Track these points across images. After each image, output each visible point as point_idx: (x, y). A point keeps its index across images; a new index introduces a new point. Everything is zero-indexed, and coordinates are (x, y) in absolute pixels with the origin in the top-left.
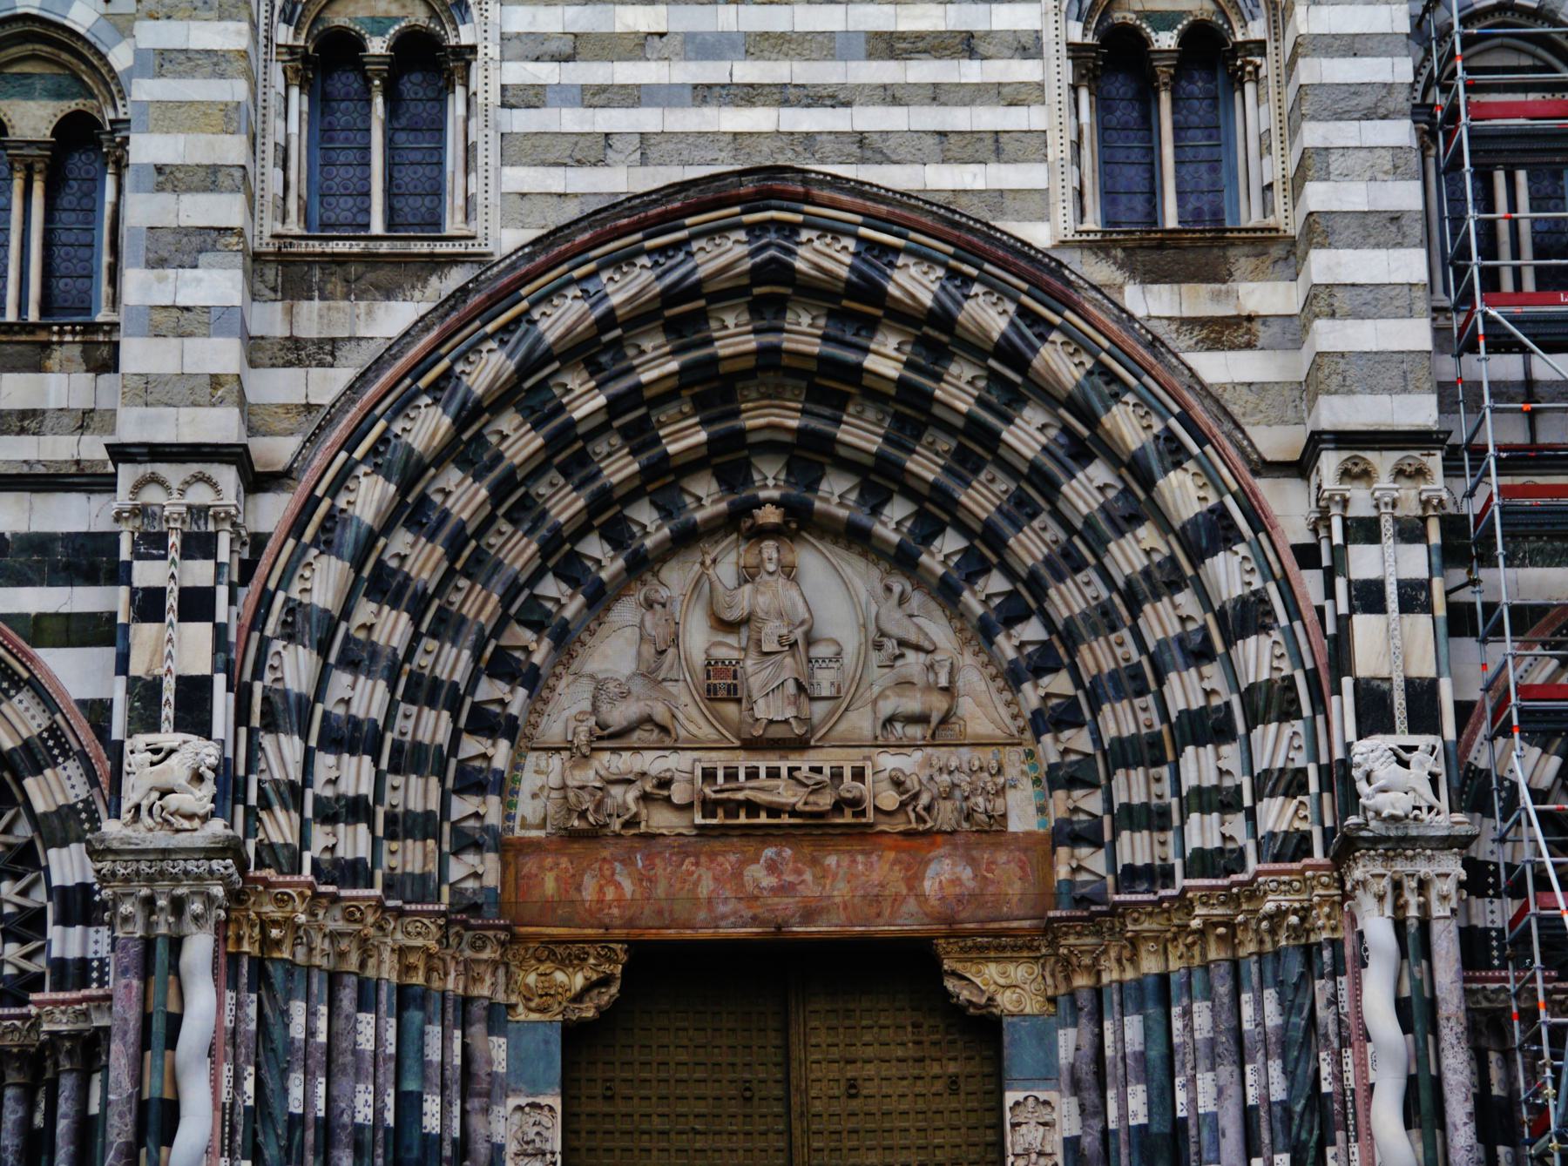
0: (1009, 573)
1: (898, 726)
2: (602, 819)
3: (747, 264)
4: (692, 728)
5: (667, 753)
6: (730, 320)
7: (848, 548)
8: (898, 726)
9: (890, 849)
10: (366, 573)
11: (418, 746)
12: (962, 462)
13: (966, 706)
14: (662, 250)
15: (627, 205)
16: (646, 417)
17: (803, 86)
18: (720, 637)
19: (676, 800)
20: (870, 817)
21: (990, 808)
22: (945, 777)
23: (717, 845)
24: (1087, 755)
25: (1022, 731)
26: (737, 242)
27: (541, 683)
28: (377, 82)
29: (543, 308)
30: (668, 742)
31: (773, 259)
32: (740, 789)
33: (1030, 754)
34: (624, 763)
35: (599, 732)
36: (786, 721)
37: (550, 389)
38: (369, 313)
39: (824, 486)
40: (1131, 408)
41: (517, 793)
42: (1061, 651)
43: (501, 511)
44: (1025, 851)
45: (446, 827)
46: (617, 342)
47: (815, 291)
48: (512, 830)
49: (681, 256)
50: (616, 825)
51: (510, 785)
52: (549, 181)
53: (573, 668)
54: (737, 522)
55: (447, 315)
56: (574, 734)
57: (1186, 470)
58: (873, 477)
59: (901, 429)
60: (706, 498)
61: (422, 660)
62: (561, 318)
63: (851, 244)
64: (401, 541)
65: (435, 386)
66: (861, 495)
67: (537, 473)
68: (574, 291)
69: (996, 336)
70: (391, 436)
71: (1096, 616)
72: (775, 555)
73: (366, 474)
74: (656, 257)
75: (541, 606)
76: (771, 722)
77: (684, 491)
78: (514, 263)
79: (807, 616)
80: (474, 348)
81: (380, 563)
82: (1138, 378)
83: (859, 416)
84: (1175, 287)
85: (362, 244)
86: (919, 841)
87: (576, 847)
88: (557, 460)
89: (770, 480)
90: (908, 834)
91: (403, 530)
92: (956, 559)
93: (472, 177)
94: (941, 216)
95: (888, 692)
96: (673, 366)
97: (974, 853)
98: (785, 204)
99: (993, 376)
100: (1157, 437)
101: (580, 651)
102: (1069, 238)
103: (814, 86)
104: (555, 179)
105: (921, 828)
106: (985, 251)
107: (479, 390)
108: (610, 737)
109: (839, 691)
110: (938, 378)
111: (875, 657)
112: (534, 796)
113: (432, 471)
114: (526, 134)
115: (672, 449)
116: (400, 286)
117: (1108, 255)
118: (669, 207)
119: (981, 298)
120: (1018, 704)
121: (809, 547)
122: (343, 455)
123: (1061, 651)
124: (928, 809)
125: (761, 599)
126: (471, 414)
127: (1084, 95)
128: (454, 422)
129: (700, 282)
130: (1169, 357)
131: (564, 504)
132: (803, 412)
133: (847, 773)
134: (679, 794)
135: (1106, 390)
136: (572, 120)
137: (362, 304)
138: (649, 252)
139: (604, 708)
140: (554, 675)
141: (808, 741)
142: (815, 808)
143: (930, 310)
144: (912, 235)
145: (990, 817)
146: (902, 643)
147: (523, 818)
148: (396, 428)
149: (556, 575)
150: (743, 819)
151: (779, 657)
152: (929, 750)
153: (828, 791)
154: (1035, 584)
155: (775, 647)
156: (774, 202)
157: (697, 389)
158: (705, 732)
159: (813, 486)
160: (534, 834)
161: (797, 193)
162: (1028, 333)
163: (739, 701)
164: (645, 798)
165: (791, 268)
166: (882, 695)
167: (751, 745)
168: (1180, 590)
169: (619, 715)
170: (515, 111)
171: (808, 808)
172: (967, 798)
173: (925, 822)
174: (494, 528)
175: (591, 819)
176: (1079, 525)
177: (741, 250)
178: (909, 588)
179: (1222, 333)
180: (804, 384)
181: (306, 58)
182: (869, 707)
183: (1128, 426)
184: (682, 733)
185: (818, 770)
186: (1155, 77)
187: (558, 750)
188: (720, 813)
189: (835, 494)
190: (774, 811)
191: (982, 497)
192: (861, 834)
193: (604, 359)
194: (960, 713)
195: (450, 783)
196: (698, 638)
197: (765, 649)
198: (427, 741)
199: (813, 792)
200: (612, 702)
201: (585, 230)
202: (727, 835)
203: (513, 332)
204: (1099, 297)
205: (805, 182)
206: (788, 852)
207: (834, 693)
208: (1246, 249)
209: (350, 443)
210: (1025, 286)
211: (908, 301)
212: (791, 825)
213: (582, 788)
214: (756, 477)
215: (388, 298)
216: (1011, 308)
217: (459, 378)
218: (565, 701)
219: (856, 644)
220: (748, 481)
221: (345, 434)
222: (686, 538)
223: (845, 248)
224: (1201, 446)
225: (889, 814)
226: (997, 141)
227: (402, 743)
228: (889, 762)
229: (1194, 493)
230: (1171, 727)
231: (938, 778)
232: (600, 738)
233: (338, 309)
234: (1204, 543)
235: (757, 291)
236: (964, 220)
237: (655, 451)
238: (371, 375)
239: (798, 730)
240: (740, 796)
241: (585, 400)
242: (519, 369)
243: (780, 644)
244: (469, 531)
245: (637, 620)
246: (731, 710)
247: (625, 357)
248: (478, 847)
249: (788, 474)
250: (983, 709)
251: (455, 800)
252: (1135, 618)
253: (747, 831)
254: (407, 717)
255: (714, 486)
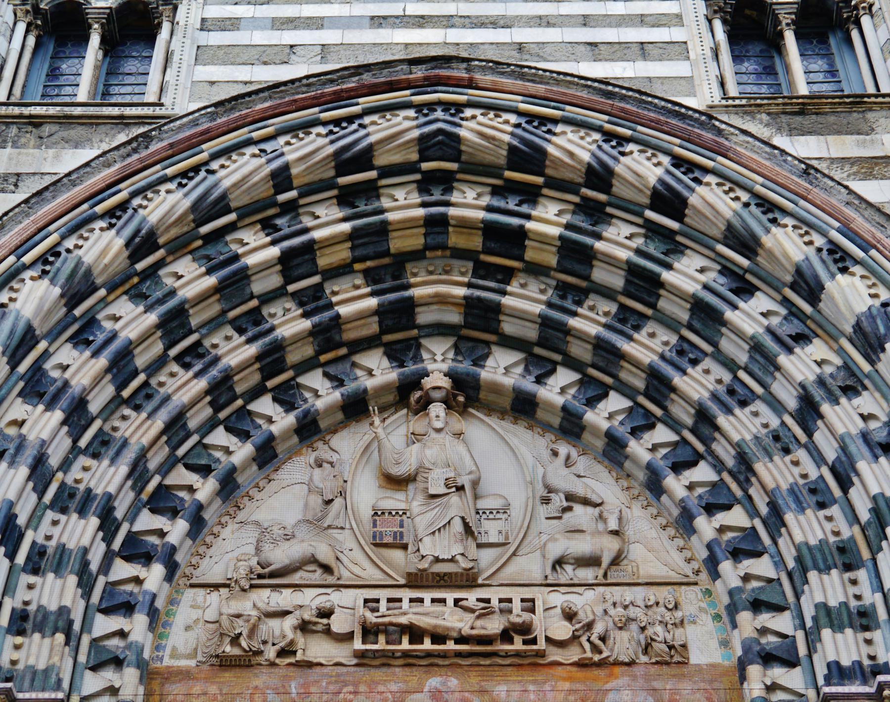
0: (673, 424)
1: (569, 568)
2: (256, 645)
3: (416, 133)
4: (357, 570)
5: (329, 591)
6: (400, 194)
7: (515, 423)
8: (569, 568)
9: (564, 679)
10: (23, 368)
11: (62, 549)
12: (623, 321)
13: (636, 552)
14: (337, 122)
15: (305, 81)
16: (318, 289)
17: (468, 17)
18: (389, 493)
19: (335, 628)
20: (542, 644)
21: (669, 637)
22: (620, 610)
23: (378, 674)
24: (770, 581)
25: (697, 572)
26: (406, 118)
27: (205, 530)
28: (96, 26)
29: (222, 161)
30: (331, 580)
31: (440, 131)
32: (405, 614)
33: (708, 593)
34: (284, 599)
35: (260, 570)
36: (452, 560)
37: (226, 244)
38: (57, 157)
39: (490, 362)
40: (790, 229)
41: (170, 625)
42: (734, 486)
43: (173, 352)
44: (711, 682)
45: (86, 640)
46: (291, 208)
47: (477, 169)
48: (161, 659)
49: (354, 126)
50: (271, 653)
51: (163, 618)
52: (237, 74)
53: (241, 516)
54: (407, 395)
55: (129, 155)
56: (236, 569)
57: (853, 274)
58: (538, 350)
59: (563, 297)
60: (377, 371)
61: (75, 472)
62: (242, 172)
63: (513, 118)
64: (66, 354)
65: (111, 213)
66: (527, 369)
67: (213, 324)
68: (254, 150)
69: (652, 181)
70: (61, 249)
71: (769, 441)
72: (442, 414)
73: (32, 279)
74: (331, 127)
75: (210, 455)
76: (437, 560)
77: (354, 365)
78: (197, 119)
79: (474, 468)
80: (153, 186)
81: (37, 368)
82: (796, 205)
83: (523, 286)
84: (821, 138)
85: (58, 108)
86: (596, 672)
87: (228, 675)
88: (232, 314)
89: (438, 362)
90: (582, 664)
91: (69, 346)
92: (620, 418)
93: (168, 70)
94: (595, 88)
95: (557, 536)
96: (346, 227)
97: (656, 684)
98: (451, 89)
99: (653, 230)
100: (819, 250)
101: (248, 504)
102: (716, 103)
103: (477, 17)
104: (243, 73)
105: (597, 658)
106: (638, 115)
107: (153, 219)
108: (271, 576)
109: (507, 538)
110: (599, 237)
111: (543, 511)
112: (188, 628)
113: (102, 292)
114: (219, 47)
115: (344, 310)
116: (90, 140)
117: (754, 118)
118: (344, 87)
119: (636, 155)
120: (690, 549)
121: (476, 422)
122: (12, 259)
123: (734, 486)
124: (603, 639)
125: (428, 452)
126: (142, 244)
127: (718, 25)
128: (127, 245)
129: (370, 148)
130: (826, 180)
131: (235, 352)
132: (469, 285)
133: (517, 606)
134: (338, 624)
135: (764, 218)
136: (260, 37)
137: (51, 152)
138: (324, 124)
139: (266, 547)
140: (220, 523)
141: (475, 579)
142: (483, 632)
143: (589, 164)
144: (568, 108)
145: (671, 647)
146: (570, 497)
147: (174, 649)
148: (69, 243)
149: (228, 429)
150: (405, 645)
151: (446, 499)
152: (601, 589)
153: (496, 617)
154: (704, 420)
155: (442, 490)
156: (440, 88)
157: (369, 264)
158: (372, 575)
159: (479, 361)
160: (183, 663)
161: (462, 79)
162: (685, 178)
163: (405, 547)
164: (304, 627)
165: (457, 138)
166: (552, 539)
167: (416, 580)
168: (857, 393)
169: (280, 555)
170: (210, 33)
171: (474, 632)
172: (643, 629)
173: (600, 652)
174: (166, 370)
175: (244, 644)
176: (742, 358)
177: (408, 124)
178: (574, 453)
179: (873, 168)
180: (470, 265)
181: (36, 10)
182: (538, 553)
183: (787, 244)
184: (346, 574)
185: (488, 601)
186: (778, 22)
187: (216, 587)
188: (382, 638)
189: (501, 369)
190: (439, 638)
191: (646, 347)
192: (532, 662)
193: (279, 222)
194: (631, 556)
195: (95, 598)
196: (366, 494)
197: (432, 491)
198: (71, 545)
199: (479, 617)
200: (275, 542)
201: (265, 100)
202: (389, 665)
203: (191, 179)
204: (750, 139)
205: (468, 70)
206: (453, 682)
207: (502, 540)
208: (884, 113)
209: (20, 249)
210: (678, 141)
211: (567, 160)
212: (459, 654)
213: (238, 616)
214: (425, 356)
215: (76, 147)
216: (666, 160)
217: (135, 210)
218: (228, 545)
219: (524, 500)
220: (417, 358)
221: (16, 241)
222: (355, 408)
223: (507, 122)
224: (866, 251)
225: (561, 644)
226: (643, 49)
227: (44, 547)
228: (558, 599)
229: (865, 292)
230: (863, 530)
231: (612, 611)
232: (260, 576)
233: (27, 155)
234: (882, 330)
235: (425, 166)
236: (617, 90)
237: (327, 315)
238: (47, 194)
239: (464, 564)
240: (403, 620)
241: (257, 249)
242: (194, 207)
243: (447, 486)
244: (141, 360)
245: (306, 479)
246: (397, 555)
247: (301, 222)
248: (118, 662)
249: (456, 354)
250: (654, 551)
251: (99, 618)
252: (810, 435)
253: (409, 659)
254: (55, 523)
255: (385, 363)
